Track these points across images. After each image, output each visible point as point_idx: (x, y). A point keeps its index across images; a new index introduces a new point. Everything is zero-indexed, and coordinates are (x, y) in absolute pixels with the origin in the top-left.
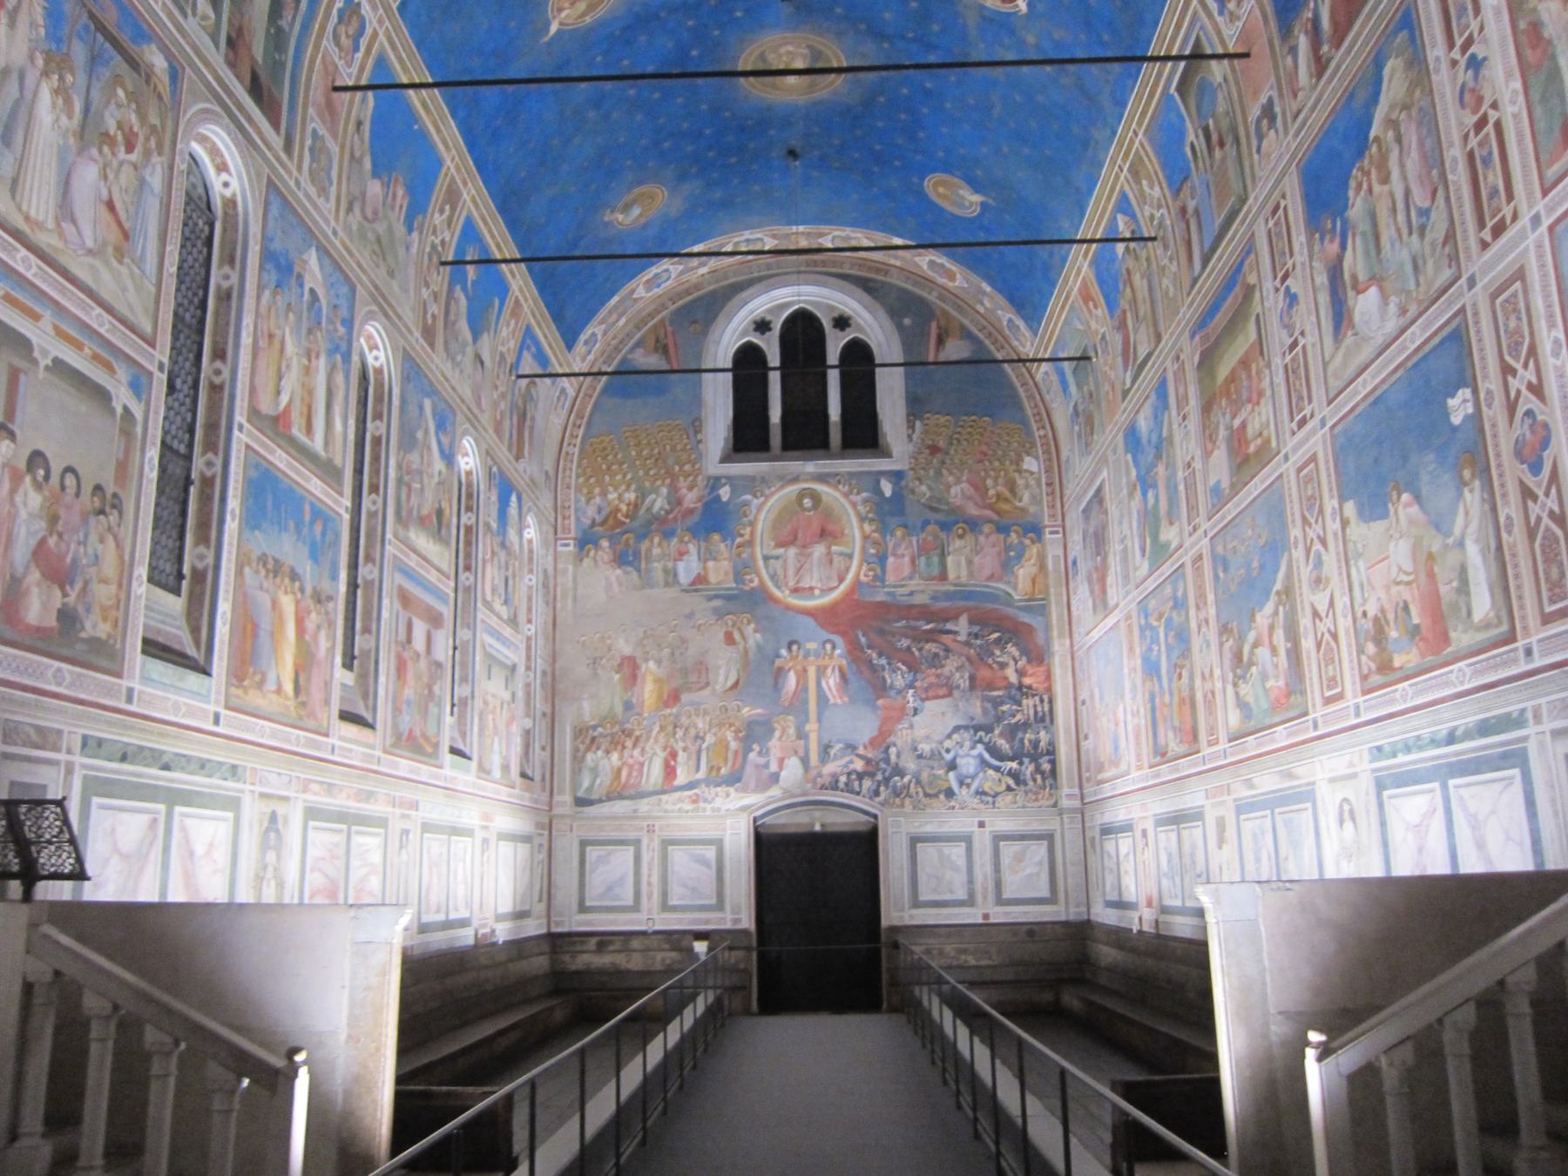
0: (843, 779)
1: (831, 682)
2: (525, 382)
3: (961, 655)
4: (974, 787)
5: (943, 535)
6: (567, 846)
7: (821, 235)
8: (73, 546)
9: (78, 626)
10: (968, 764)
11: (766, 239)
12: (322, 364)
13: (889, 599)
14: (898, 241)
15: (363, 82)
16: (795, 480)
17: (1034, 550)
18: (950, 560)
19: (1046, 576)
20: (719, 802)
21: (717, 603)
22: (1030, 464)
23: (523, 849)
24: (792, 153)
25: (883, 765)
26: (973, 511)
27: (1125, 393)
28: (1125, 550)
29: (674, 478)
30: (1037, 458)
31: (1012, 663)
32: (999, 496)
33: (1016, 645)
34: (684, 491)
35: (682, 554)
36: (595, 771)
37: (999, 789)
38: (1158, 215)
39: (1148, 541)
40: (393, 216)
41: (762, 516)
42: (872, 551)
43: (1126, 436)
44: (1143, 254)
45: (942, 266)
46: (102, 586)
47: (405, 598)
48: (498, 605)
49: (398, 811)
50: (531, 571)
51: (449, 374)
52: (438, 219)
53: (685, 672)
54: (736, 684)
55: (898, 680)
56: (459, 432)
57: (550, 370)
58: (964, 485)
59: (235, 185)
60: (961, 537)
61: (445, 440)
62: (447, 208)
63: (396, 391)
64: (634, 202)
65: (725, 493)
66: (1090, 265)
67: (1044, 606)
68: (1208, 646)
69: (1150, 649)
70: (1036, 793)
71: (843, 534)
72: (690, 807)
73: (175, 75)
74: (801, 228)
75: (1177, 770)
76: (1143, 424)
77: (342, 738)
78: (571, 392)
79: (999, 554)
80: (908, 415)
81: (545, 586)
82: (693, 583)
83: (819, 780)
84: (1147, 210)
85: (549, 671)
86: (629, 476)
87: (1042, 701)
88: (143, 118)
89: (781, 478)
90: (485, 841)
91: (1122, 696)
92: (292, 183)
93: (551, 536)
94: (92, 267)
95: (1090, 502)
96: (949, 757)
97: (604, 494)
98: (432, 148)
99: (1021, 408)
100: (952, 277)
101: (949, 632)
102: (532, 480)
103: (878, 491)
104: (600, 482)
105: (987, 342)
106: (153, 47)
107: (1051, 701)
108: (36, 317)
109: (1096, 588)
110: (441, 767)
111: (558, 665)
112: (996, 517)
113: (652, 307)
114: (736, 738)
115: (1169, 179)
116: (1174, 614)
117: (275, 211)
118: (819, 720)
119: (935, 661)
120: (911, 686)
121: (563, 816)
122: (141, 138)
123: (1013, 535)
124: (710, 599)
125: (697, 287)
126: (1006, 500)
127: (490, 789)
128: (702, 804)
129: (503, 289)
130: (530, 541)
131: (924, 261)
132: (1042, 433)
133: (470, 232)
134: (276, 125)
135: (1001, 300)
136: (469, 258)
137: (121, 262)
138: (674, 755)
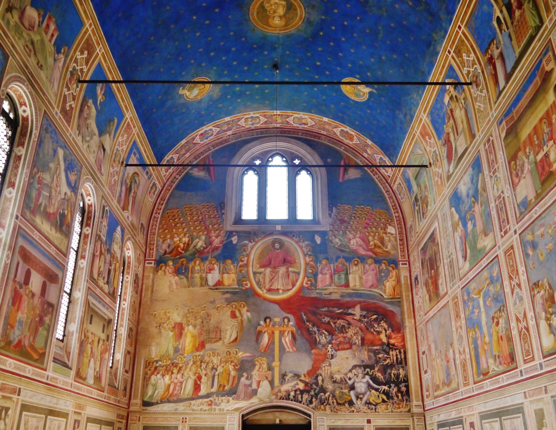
0: (292, 394)
1: (287, 339)
2: (131, 170)
3: (356, 326)
4: (365, 399)
5: (347, 264)
7: (288, 116)
10: (361, 387)
11: (261, 117)
13: (319, 296)
16: (271, 234)
18: (351, 277)
19: (400, 286)
20: (223, 406)
22: (391, 230)
25: (315, 387)
26: (362, 252)
27: (449, 177)
29: (209, 231)
30: (394, 227)
31: (384, 331)
32: (375, 245)
33: (386, 322)
34: (214, 238)
35: (211, 270)
37: (378, 401)
38: (471, 70)
39: (468, 251)
42: (310, 271)
43: (450, 200)
45: (347, 132)
47: (25, 256)
48: (101, 283)
50: (128, 273)
51: (80, 143)
52: (78, 55)
53: (208, 332)
54: (236, 339)
55: (323, 339)
56: (83, 178)
58: (357, 239)
60: (356, 265)
61: (73, 178)
65: (235, 240)
66: (427, 116)
67: (400, 301)
68: (521, 299)
69: (473, 312)
70: (399, 404)
71: (295, 262)
72: (207, 408)
74: (278, 112)
75: (499, 382)
76: (463, 189)
78: (159, 187)
79: (376, 274)
82: (216, 285)
83: (279, 394)
85: (134, 329)
86: (186, 230)
87: (400, 352)
89: (264, 233)
90: (77, 422)
91: (451, 345)
93: (142, 258)
96: (350, 382)
97: (172, 238)
99: (386, 203)
100: (351, 139)
101: (351, 314)
103: (313, 241)
104: (171, 232)
107: (405, 353)
109: (431, 288)
111: (139, 327)
112: (374, 256)
113: (204, 149)
114: (235, 369)
115: (480, 47)
116: (491, 288)
118: (280, 360)
119: (343, 330)
120: (330, 342)
123: (383, 265)
124: (224, 293)
125: (226, 141)
126: (379, 247)
127: (84, 389)
130: (129, 257)
132: (397, 215)
135: (378, 149)
138: (200, 378)
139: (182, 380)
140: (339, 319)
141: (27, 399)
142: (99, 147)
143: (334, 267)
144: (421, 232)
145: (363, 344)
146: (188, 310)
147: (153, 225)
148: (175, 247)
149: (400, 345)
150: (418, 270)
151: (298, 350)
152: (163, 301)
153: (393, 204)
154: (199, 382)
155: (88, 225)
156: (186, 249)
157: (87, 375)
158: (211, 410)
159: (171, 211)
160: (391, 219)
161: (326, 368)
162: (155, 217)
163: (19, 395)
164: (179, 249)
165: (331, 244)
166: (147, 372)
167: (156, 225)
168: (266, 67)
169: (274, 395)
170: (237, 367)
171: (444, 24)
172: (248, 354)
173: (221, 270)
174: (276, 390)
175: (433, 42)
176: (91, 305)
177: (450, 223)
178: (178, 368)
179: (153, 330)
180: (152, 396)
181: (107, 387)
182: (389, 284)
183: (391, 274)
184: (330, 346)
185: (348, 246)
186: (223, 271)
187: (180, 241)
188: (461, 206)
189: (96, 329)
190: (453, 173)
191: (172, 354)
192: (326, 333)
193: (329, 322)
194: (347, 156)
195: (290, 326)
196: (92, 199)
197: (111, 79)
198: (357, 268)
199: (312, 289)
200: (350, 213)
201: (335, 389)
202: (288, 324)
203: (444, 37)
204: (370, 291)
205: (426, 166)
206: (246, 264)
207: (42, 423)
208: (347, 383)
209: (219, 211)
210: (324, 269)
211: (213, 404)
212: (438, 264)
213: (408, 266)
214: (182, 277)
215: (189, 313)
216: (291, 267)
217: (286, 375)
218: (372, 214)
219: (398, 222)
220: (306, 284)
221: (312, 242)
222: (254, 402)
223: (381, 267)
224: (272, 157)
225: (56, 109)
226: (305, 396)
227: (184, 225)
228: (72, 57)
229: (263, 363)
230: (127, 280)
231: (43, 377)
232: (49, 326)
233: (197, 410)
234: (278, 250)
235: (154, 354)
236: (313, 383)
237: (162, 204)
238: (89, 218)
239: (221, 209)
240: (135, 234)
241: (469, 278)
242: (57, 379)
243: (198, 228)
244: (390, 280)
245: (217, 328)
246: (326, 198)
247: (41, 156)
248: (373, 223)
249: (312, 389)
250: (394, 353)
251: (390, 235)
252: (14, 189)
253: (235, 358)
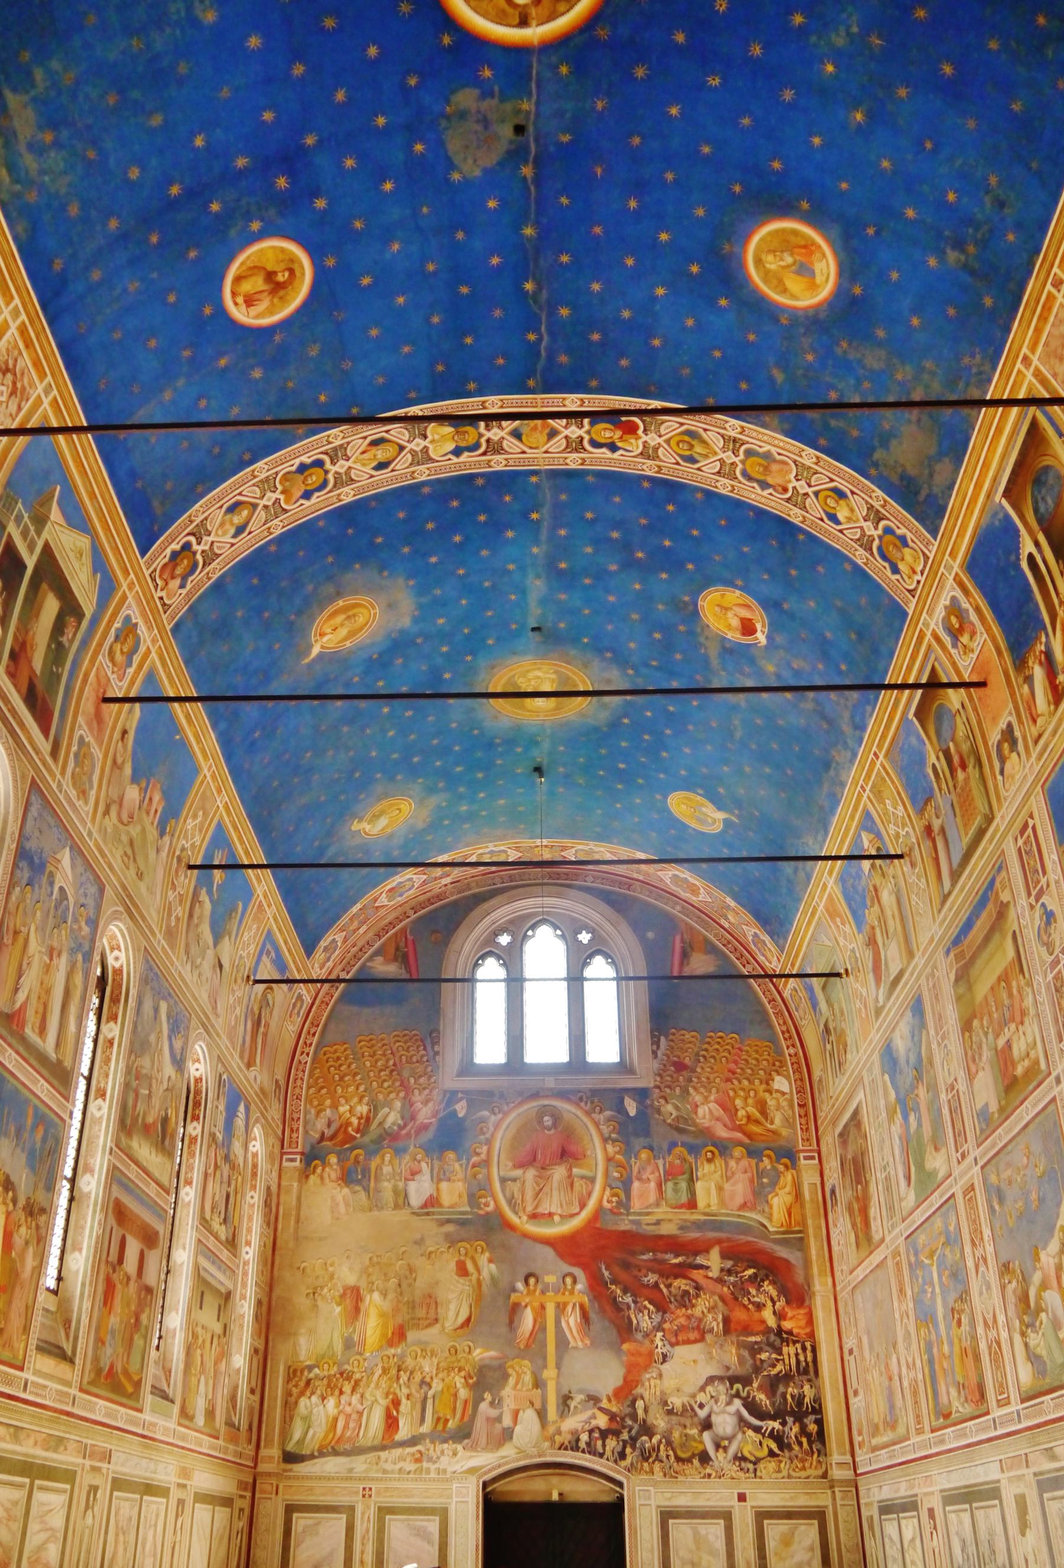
0: (584, 1437)
2: (263, 986)
3: (713, 1293)
5: (691, 1159)
6: (271, 1511)
7: (564, 848)
10: (725, 1422)
12: (62, 963)
13: (634, 1228)
14: (642, 856)
15: (132, 695)
16: (535, 1095)
17: (788, 1177)
18: (699, 1186)
19: (802, 1206)
20: (444, 1462)
21: (450, 1228)
22: (781, 1083)
23: (222, 1514)
24: (538, 770)
25: (629, 1422)
26: (722, 1132)
27: (878, 1011)
28: (888, 1179)
30: (788, 1078)
31: (769, 1304)
32: (749, 1117)
33: (773, 1283)
35: (414, 1173)
36: (307, 1420)
40: (147, 820)
41: (499, 1135)
42: (616, 1174)
43: (882, 1057)
44: (891, 871)
47: (120, 1213)
48: (216, 1225)
49: (88, 1463)
50: (253, 1187)
51: (188, 977)
53: (412, 1305)
55: (645, 1321)
56: (193, 1035)
57: (288, 975)
58: (713, 1105)
60: (709, 1161)
61: (178, 1044)
62: (201, 813)
63: (133, 992)
64: (382, 813)
65: (461, 1109)
66: (835, 883)
67: (802, 1239)
72: (413, 1467)
74: (545, 842)
76: (901, 1045)
77: (37, 1373)
78: (308, 999)
79: (752, 1181)
80: (652, 1032)
81: (267, 1204)
84: (892, 831)
85: (265, 1301)
86: (362, 1088)
90: (181, 1502)
92: (54, 786)
93: (277, 1150)
95: (845, 1127)
96: (702, 1414)
97: (335, 1106)
98: (191, 756)
99: (770, 1026)
101: (700, 1267)
102: (262, 1089)
103: (621, 1109)
104: (332, 1094)
105: (731, 956)
109: (858, 1220)
110: (140, 1411)
111: (274, 1295)
112: (747, 1141)
115: (913, 800)
117: (34, 811)
118: (558, 1366)
119: (685, 1300)
120: (659, 1328)
121: (269, 1474)
125: (439, 897)
126: (757, 1122)
128: (425, 1465)
129: (248, 893)
131: (667, 874)
132: (792, 1051)
133: (220, 838)
134: (45, 731)
135: (749, 918)
136: (216, 862)
138: (396, 1403)
139: (360, 1408)
140: (676, 1277)
141: (119, 1469)
142: (214, 966)
143: (664, 1165)
144: (837, 1100)
145: (727, 1331)
146: (371, 1259)
147: (296, 1080)
148: (341, 1127)
149: (802, 1332)
150: (836, 1175)
151: (594, 1345)
152: (321, 1239)
153: (784, 1028)
154: (395, 1413)
155: (196, 1118)
156: (362, 1130)
157: (195, 1409)
158: (419, 1471)
159: (332, 1050)
160: (780, 1061)
161: (652, 1382)
162: (300, 1062)
163: (109, 1463)
164: (350, 1129)
165: (657, 1116)
166: (291, 1391)
167: (302, 1079)
168: (519, 771)
169: (546, 1439)
170: (471, 1381)
171: (850, 742)
172: (493, 1353)
173: (435, 1172)
174: (551, 1429)
175: (834, 765)
176: (201, 1272)
177: (882, 1102)
178: (353, 1382)
179: (301, 1301)
180: (301, 1442)
181: (223, 1429)
182: (779, 1201)
183: (782, 1179)
184: (660, 1334)
185: (693, 1120)
186: (438, 1174)
187: (350, 1111)
188: (898, 1075)
189: (208, 1318)
190: (883, 1007)
191: (340, 1353)
192: (651, 1307)
193: (656, 1283)
194: (687, 924)
195: (576, 1292)
196: (201, 1067)
197: (246, 863)
198: (713, 1166)
199: (621, 1214)
200: (696, 1050)
201: (672, 1428)
202: (573, 1288)
203: (852, 761)
204: (739, 1216)
205: (838, 975)
206: (485, 1161)
207: (137, 1509)
208: (696, 1414)
209: (429, 1047)
210: (644, 1169)
211: (425, 1458)
212: (867, 1176)
213: (816, 1161)
214: (358, 1188)
215: (372, 1265)
216: (577, 1166)
217: (571, 1398)
218: (740, 1049)
219: (795, 1066)
220: (608, 1202)
221: (619, 1112)
222: (508, 1456)
223: (762, 1165)
224: (533, 927)
225: (158, 934)
226: (611, 1443)
227: (358, 1077)
228: (181, 832)
229: (522, 1371)
230: (252, 1202)
231: (136, 1424)
232: (147, 1328)
233: (392, 1472)
234: (549, 1130)
235: (303, 1352)
236: (626, 1415)
237: (314, 1035)
238: (197, 1104)
239: (433, 1044)
240: (265, 1108)
241: (914, 1221)
242: (154, 1425)
243: (386, 1085)
244: (780, 1192)
245: (430, 1297)
246: (646, 1017)
247: (139, 1028)
248: (742, 1069)
249: (624, 1427)
250: (792, 1350)
251: (779, 1095)
252: (104, 1100)
253: (467, 1361)
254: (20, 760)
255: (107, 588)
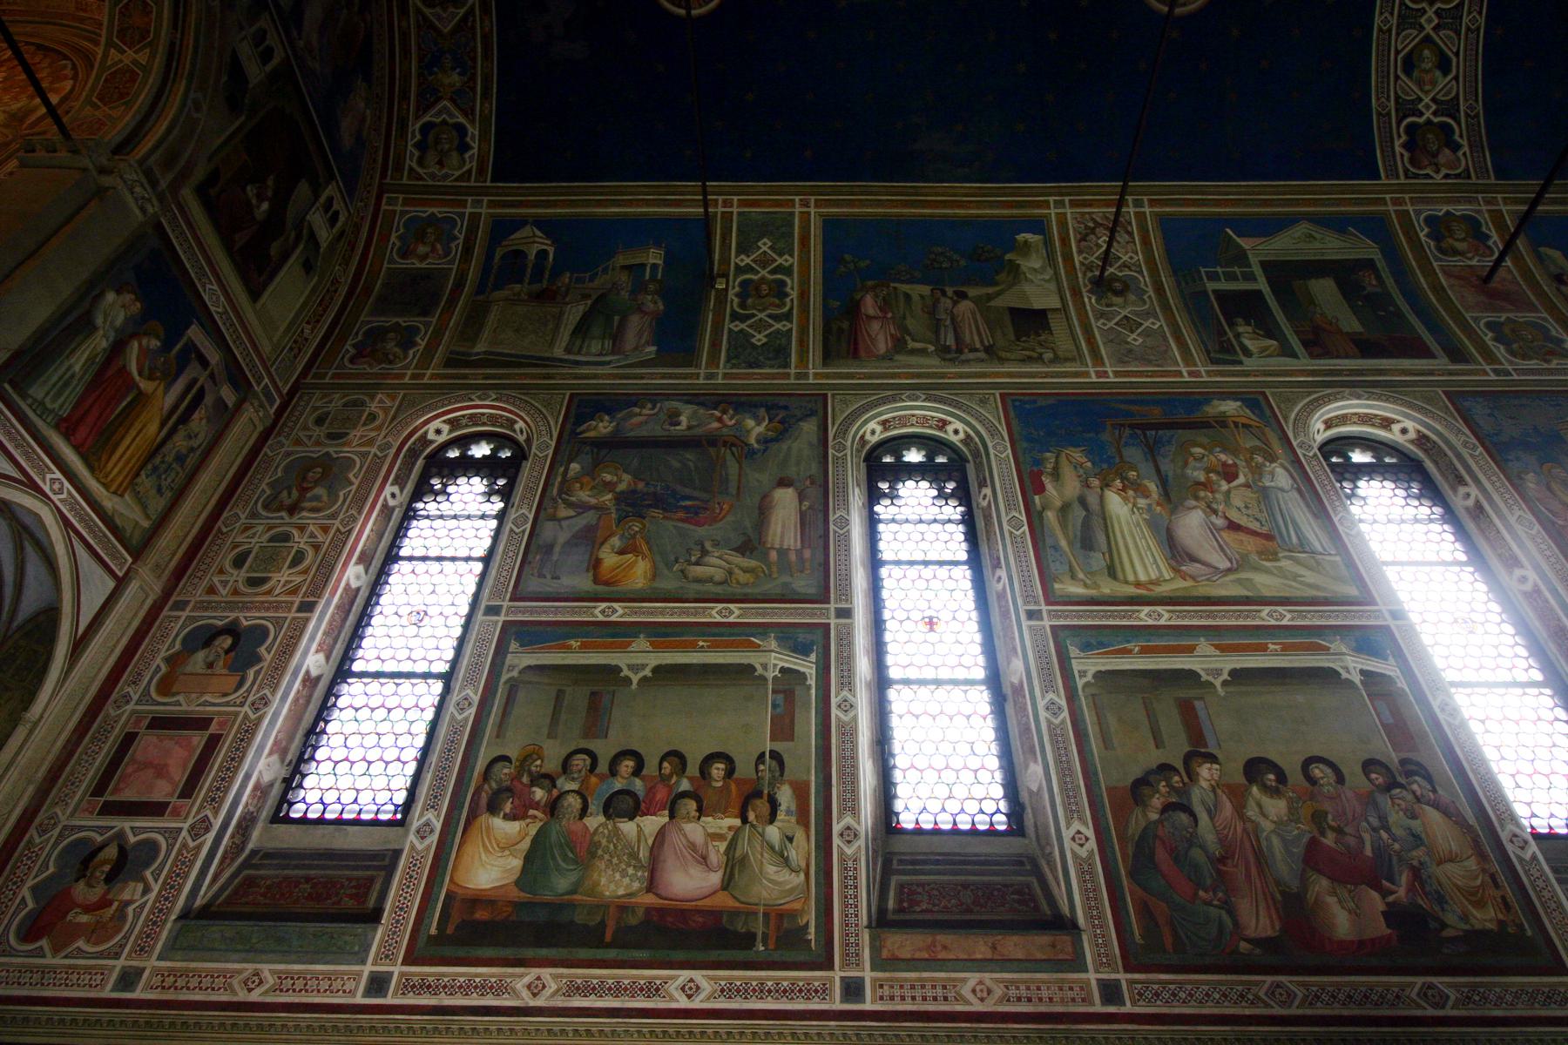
8: (1367, 837)
9: (1433, 925)
46: (1449, 867)
59: (1409, 425)
73: (1254, 402)
88: (1235, 452)
94: (1239, 581)
106: (1216, 402)
108: (1190, 650)
122: (1241, 464)
137: (1277, 560)
254: (1400, 393)
255: (1375, 227)
